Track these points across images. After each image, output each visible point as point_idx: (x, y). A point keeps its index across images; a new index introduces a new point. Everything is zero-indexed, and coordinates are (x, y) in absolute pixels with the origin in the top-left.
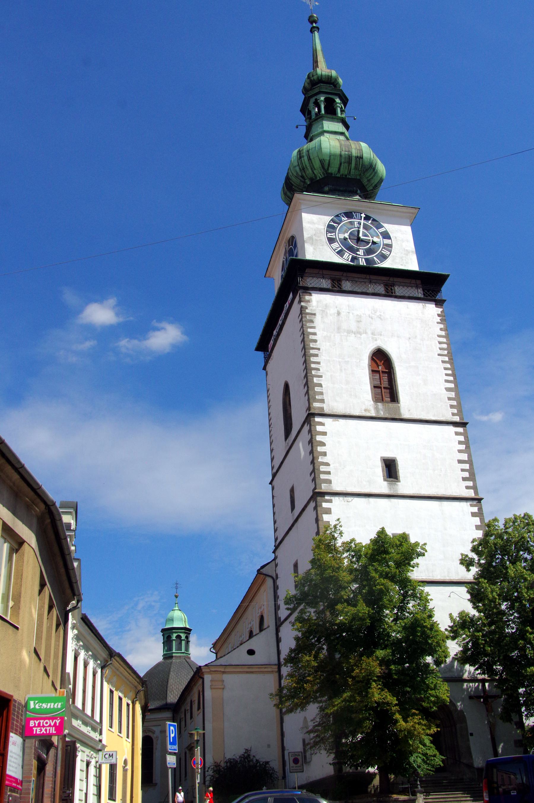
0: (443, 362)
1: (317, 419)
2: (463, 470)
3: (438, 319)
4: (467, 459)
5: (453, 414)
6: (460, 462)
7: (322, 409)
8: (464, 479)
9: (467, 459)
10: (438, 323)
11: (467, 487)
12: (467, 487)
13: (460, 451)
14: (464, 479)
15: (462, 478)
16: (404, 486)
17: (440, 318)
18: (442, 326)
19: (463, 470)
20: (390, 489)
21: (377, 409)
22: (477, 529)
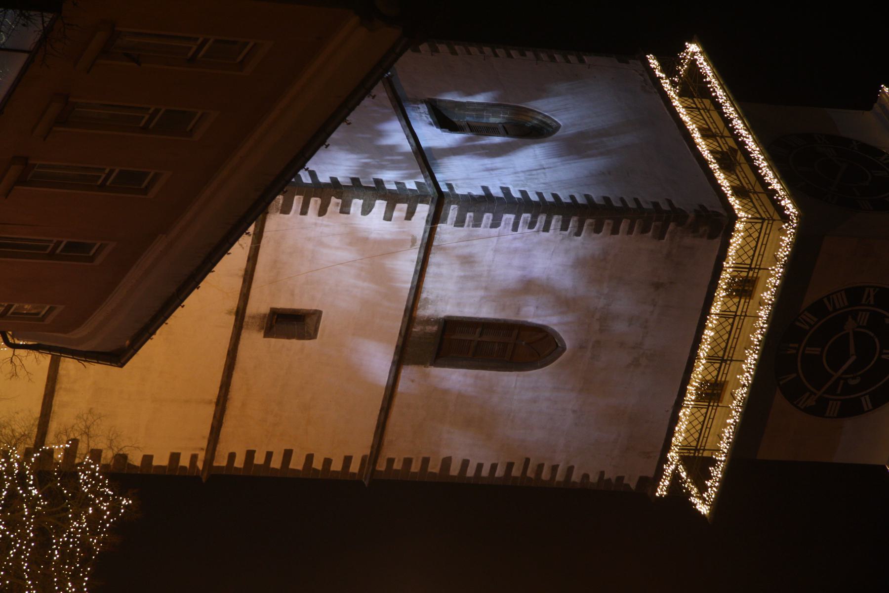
0: (510, 466)
1: (423, 210)
2: (269, 455)
3: (609, 475)
4: (291, 466)
5: (391, 461)
6: (288, 454)
7: (444, 220)
8: (250, 454)
9: (291, 466)
10: (602, 473)
11: (232, 456)
12: (232, 456)
13: (310, 458)
14: (250, 454)
15: (254, 452)
16: (254, 342)
17: (613, 480)
18: (594, 478)
19: (269, 455)
20: (253, 317)
21: (428, 321)
22: (145, 457)
